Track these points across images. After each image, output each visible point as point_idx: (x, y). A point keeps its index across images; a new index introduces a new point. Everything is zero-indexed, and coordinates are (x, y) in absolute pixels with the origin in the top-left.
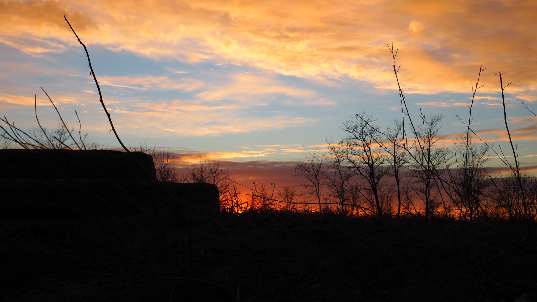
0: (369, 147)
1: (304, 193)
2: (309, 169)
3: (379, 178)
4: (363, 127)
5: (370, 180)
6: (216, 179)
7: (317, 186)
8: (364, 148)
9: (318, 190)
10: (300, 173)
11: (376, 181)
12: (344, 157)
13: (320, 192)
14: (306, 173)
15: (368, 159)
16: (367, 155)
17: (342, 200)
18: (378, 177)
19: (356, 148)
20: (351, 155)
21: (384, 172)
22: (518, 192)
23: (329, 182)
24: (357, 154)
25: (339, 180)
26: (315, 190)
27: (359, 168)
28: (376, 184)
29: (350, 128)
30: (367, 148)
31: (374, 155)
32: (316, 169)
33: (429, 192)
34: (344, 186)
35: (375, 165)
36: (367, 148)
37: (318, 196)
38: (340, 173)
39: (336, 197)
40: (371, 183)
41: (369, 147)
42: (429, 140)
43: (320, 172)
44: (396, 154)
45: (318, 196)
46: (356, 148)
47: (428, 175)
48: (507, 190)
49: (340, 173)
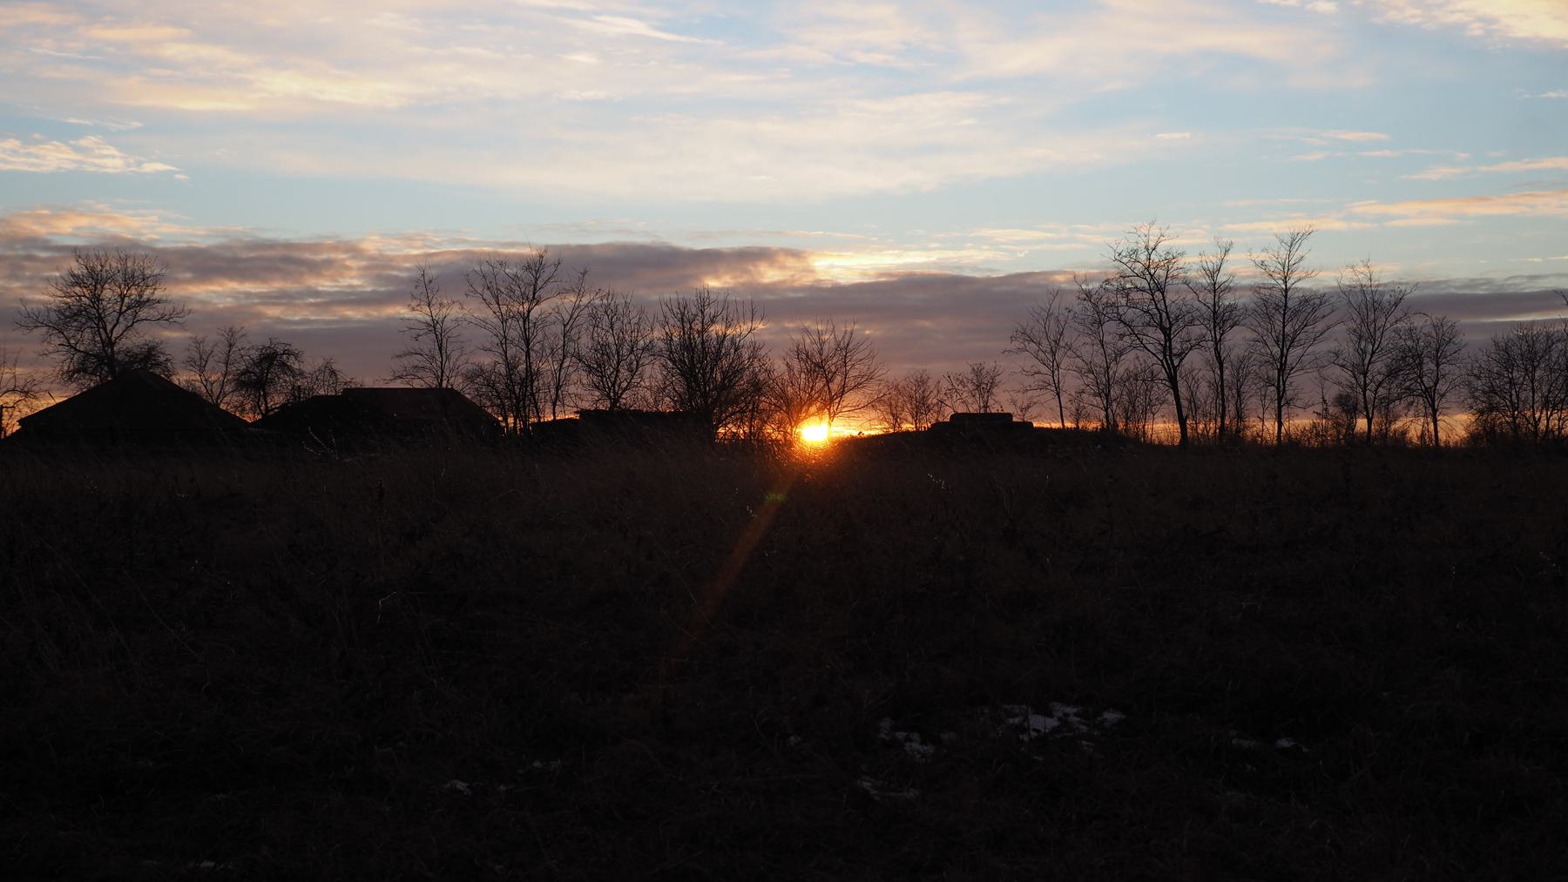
0: (1163, 293)
2: (1038, 339)
3: (1182, 355)
7: (1056, 372)
8: (1152, 295)
9: (1056, 382)
11: (1176, 363)
15: (1161, 317)
16: (1157, 307)
17: (1107, 402)
18: (1179, 355)
19: (1136, 296)
20: (1126, 308)
25: (1099, 360)
26: (1051, 381)
27: (1141, 337)
29: (1124, 254)
31: (1173, 309)
32: (1052, 338)
34: (1111, 373)
35: (1173, 329)
37: (1058, 394)
38: (1103, 345)
39: (1095, 395)
41: (1163, 293)
42: (1286, 278)
43: (1062, 343)
44: (1217, 308)
45: (1058, 394)
47: (1283, 347)
48: (1507, 370)
49: (1103, 345)
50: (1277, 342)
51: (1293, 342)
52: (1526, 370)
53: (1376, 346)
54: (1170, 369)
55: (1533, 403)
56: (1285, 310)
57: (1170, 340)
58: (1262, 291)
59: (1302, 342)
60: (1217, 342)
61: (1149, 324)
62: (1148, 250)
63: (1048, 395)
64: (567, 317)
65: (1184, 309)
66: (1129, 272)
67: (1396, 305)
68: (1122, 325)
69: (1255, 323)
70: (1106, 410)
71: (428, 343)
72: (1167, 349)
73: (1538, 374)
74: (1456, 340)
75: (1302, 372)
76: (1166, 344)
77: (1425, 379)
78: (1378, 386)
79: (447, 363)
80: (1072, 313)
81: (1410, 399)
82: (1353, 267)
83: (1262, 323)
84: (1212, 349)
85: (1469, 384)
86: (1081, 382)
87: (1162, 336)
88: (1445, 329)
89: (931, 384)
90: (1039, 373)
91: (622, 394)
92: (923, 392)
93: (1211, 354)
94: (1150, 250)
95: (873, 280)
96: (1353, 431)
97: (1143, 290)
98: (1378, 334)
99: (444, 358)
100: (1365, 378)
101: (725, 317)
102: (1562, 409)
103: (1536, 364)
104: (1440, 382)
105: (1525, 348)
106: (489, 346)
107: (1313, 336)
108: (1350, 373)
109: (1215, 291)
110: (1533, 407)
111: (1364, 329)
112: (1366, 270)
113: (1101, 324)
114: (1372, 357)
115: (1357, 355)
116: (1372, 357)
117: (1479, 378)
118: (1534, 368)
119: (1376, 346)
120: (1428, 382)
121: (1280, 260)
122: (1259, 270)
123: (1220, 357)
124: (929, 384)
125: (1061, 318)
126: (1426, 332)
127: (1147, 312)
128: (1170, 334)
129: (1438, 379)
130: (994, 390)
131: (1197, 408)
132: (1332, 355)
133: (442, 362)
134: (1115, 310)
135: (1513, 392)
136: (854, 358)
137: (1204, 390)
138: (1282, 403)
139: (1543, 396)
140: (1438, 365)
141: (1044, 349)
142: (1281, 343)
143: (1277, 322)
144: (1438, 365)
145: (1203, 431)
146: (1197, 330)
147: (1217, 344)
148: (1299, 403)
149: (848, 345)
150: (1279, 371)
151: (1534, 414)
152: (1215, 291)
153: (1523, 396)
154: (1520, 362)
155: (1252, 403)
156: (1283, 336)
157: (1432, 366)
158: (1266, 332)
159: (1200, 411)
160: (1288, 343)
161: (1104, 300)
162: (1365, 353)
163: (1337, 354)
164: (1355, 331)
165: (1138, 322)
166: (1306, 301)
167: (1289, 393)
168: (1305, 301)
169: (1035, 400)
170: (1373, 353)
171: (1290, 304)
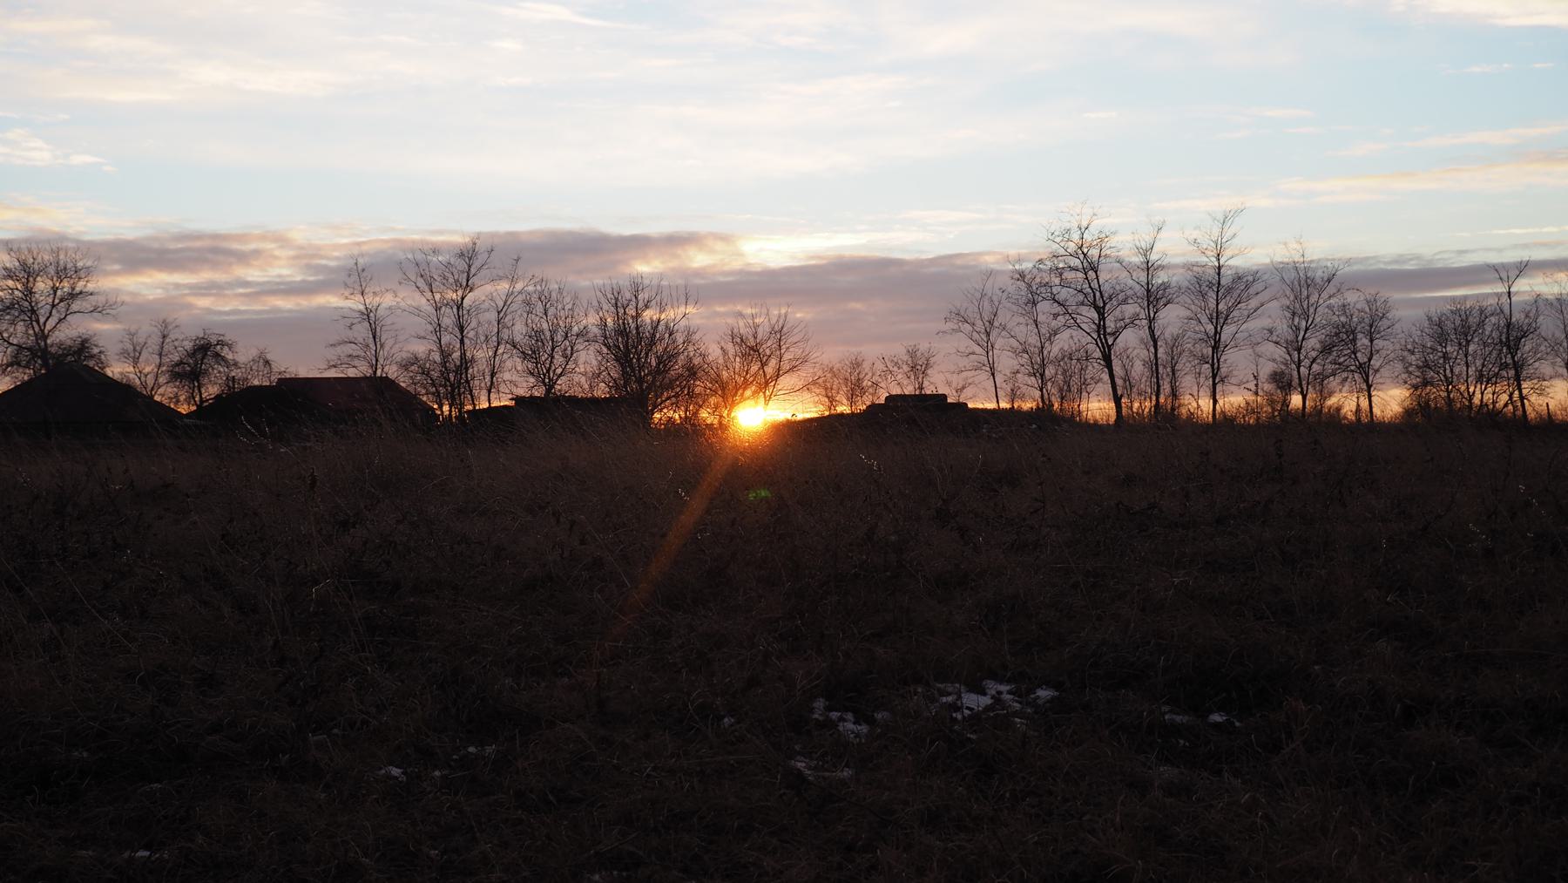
0: (1096, 272)
1: (963, 369)
3: (1116, 334)
4: (1083, 230)
5: (1098, 340)
6: (782, 344)
7: (990, 353)
9: (991, 362)
10: (956, 327)
12: (1043, 295)
13: (995, 366)
14: (968, 327)
16: (1090, 287)
17: (1042, 381)
18: (1113, 334)
19: (1069, 275)
21: (1127, 321)
22: (1467, 350)
23: (1015, 344)
24: (1072, 286)
25: (1033, 340)
26: (986, 363)
27: (1075, 316)
28: (1109, 347)
30: (1091, 274)
31: (1106, 288)
33: (1218, 361)
34: (1045, 353)
35: (1107, 308)
36: (1091, 274)
37: (993, 374)
38: (1037, 325)
39: (1030, 375)
40: (1100, 345)
41: (1096, 272)
42: (1219, 255)
43: (996, 324)
44: (1150, 286)
45: (993, 374)
46: (1069, 275)
48: (1441, 345)
49: (1037, 325)
50: (1211, 320)
51: (1226, 319)
52: (1460, 344)
53: (1310, 322)
54: (1104, 349)
55: (1467, 378)
56: (1218, 288)
57: (1104, 319)
58: (1195, 268)
59: (1236, 319)
60: (1151, 321)
61: (1082, 304)
62: (1080, 229)
63: (983, 376)
64: (501, 304)
65: (1118, 288)
66: (1062, 252)
67: (1329, 281)
68: (1056, 304)
69: (1190, 301)
70: (1041, 390)
71: (362, 331)
72: (1101, 328)
73: (1472, 348)
74: (1389, 315)
75: (1236, 349)
76: (1100, 323)
77: (1359, 355)
78: (1312, 363)
79: (381, 352)
80: (1005, 294)
81: (1345, 375)
82: (1285, 244)
83: (1196, 302)
84: (1147, 328)
85: (1403, 360)
86: (1016, 362)
87: (1096, 316)
88: (1378, 304)
89: (866, 366)
90: (973, 353)
91: (557, 380)
92: (858, 374)
93: (1145, 333)
94: (1083, 230)
95: (802, 263)
96: (1288, 406)
97: (1076, 269)
98: (1312, 310)
99: (378, 346)
100: (1299, 353)
101: (659, 302)
102: (1496, 383)
103: (1469, 338)
104: (1374, 357)
105: (1458, 322)
106: (423, 334)
107: (1246, 313)
108: (1285, 350)
109: (1148, 269)
110: (1467, 381)
111: (1297, 306)
112: (1298, 247)
113: (1034, 303)
114: (1305, 333)
115: (1290, 330)
116: (1305, 333)
117: (1413, 353)
118: (1468, 342)
119: (1310, 322)
120: (1362, 358)
121: (1212, 237)
122: (1191, 248)
123: (1154, 336)
124: (864, 366)
125: (995, 298)
126: (1360, 308)
127: (1081, 291)
128: (1104, 313)
129: (1372, 355)
130: (929, 372)
131: (1131, 387)
132: (1265, 331)
133: (376, 351)
134: (1049, 290)
135: (1447, 367)
136: (789, 341)
137: (1139, 370)
138: (1217, 379)
139: (1476, 370)
140: (1372, 341)
141: (978, 330)
142: (1214, 321)
143: (1211, 299)
144: (1372, 341)
145: (1138, 409)
146: (1130, 309)
147: (1151, 323)
148: (1233, 380)
149: (782, 328)
150: (1213, 348)
151: (1468, 388)
152: (1148, 269)
153: (1457, 370)
154: (1453, 337)
155: (1187, 382)
156: (1217, 312)
157: (1366, 342)
158: (1199, 309)
159: (1135, 390)
160: (1222, 321)
161: (1038, 280)
162: (1298, 329)
163: (1271, 331)
164: (1288, 307)
165: (1072, 301)
166: (1239, 278)
167: (1223, 371)
168: (1238, 278)
169: (970, 381)
170: (1307, 329)
171: (1223, 282)
